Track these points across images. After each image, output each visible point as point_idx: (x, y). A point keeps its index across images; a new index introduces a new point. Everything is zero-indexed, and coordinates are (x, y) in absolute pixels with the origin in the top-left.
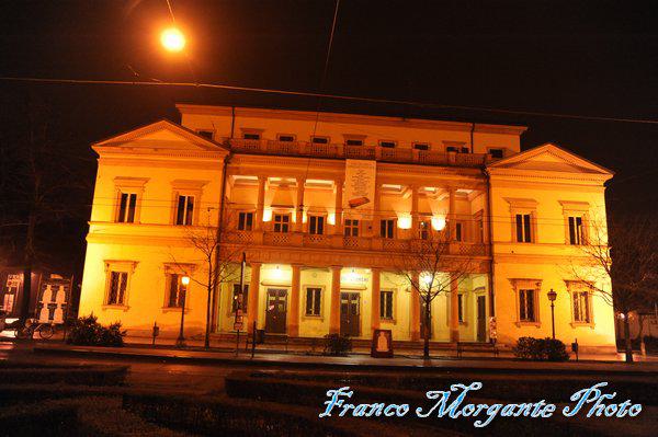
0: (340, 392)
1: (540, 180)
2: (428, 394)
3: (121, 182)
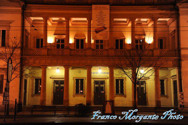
0: (97, 112)
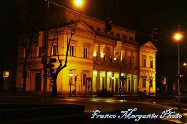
0: (97, 111)
1: (150, 51)
2: (122, 112)
3: (86, 45)
